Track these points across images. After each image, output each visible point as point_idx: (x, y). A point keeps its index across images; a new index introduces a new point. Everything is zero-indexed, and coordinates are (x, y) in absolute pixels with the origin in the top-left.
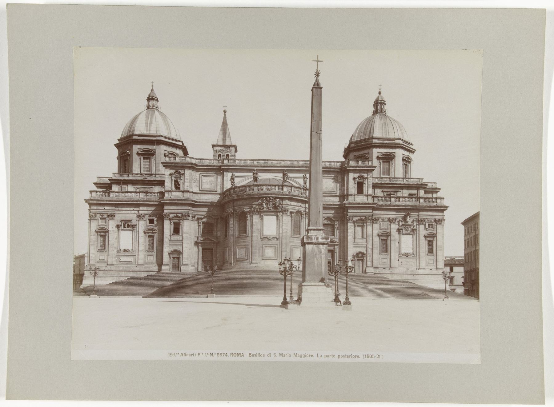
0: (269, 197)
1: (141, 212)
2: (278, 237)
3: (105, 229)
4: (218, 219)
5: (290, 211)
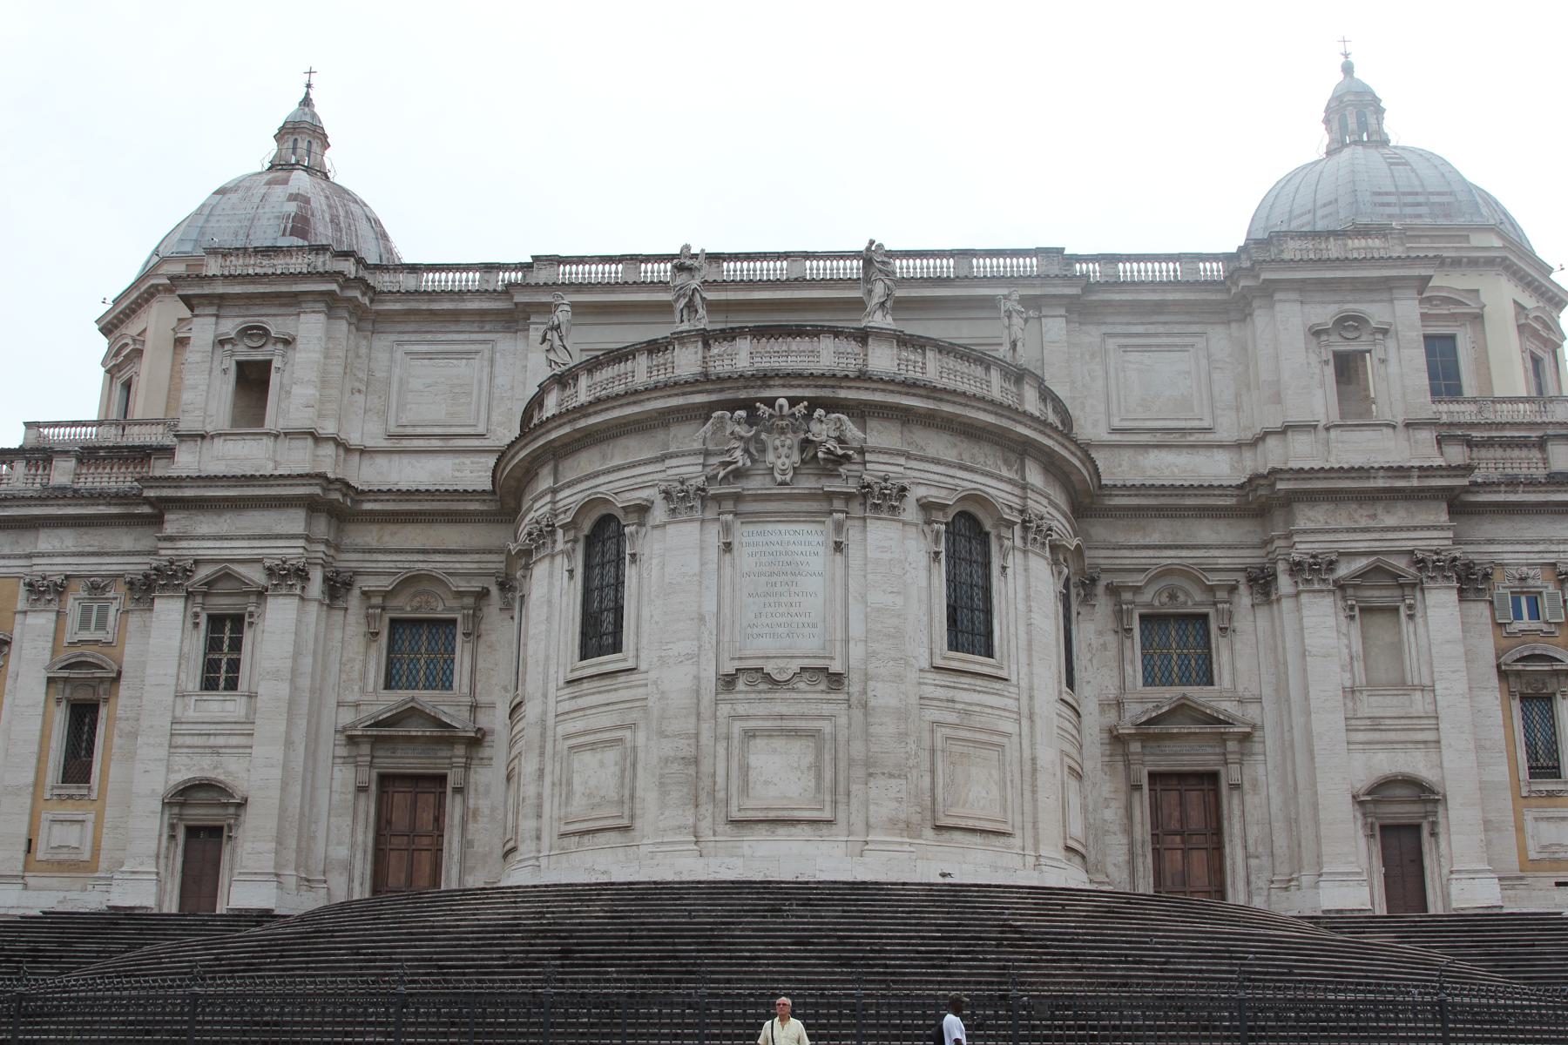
0: (770, 402)
1: (42, 566)
2: (836, 667)
4: (484, 594)
5: (921, 492)
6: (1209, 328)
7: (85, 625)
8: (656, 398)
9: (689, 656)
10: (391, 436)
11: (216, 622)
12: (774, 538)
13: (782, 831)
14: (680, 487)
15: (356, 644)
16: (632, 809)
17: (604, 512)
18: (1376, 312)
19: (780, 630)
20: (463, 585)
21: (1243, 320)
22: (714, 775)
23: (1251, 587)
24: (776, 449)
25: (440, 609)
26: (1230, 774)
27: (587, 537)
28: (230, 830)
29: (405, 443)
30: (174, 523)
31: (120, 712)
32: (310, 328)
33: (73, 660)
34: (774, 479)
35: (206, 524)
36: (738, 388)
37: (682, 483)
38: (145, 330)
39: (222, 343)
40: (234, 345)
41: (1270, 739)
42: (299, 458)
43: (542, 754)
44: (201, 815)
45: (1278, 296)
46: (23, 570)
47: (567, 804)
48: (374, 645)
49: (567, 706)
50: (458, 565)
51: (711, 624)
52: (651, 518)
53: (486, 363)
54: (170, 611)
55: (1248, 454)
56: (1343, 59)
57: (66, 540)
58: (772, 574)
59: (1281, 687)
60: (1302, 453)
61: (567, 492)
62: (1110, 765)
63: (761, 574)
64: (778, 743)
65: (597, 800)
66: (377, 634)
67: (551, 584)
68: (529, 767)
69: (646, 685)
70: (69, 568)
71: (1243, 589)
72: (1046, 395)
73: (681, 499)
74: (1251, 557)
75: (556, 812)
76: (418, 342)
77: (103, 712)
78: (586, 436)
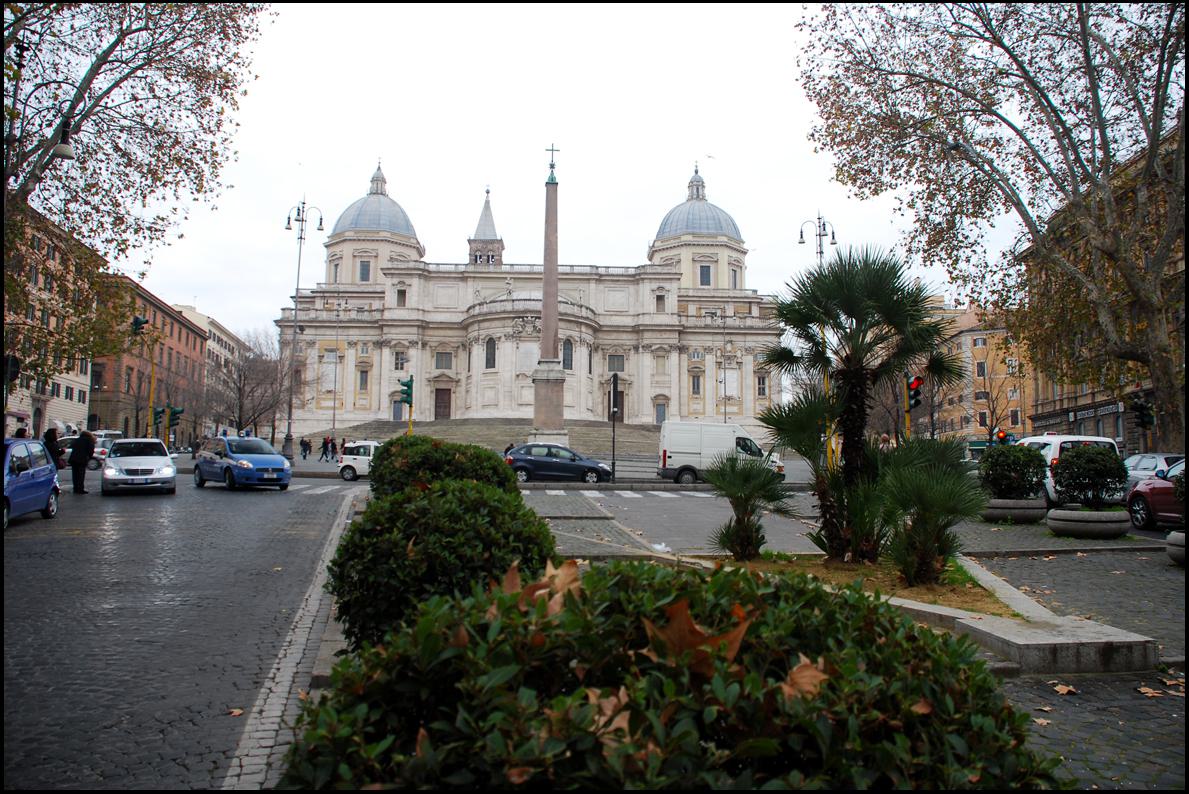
1: (351, 338)
4: (458, 347)
11: (397, 354)
15: (430, 358)
18: (667, 285)
20: (452, 345)
26: (626, 392)
30: (386, 330)
32: (415, 282)
35: (393, 330)
41: (635, 385)
42: (414, 316)
54: (386, 351)
56: (695, 168)
57: (356, 331)
59: (638, 373)
60: (646, 320)
62: (599, 389)
68: (473, 390)
72: (587, 308)
73: (508, 337)
74: (634, 343)
77: (369, 373)
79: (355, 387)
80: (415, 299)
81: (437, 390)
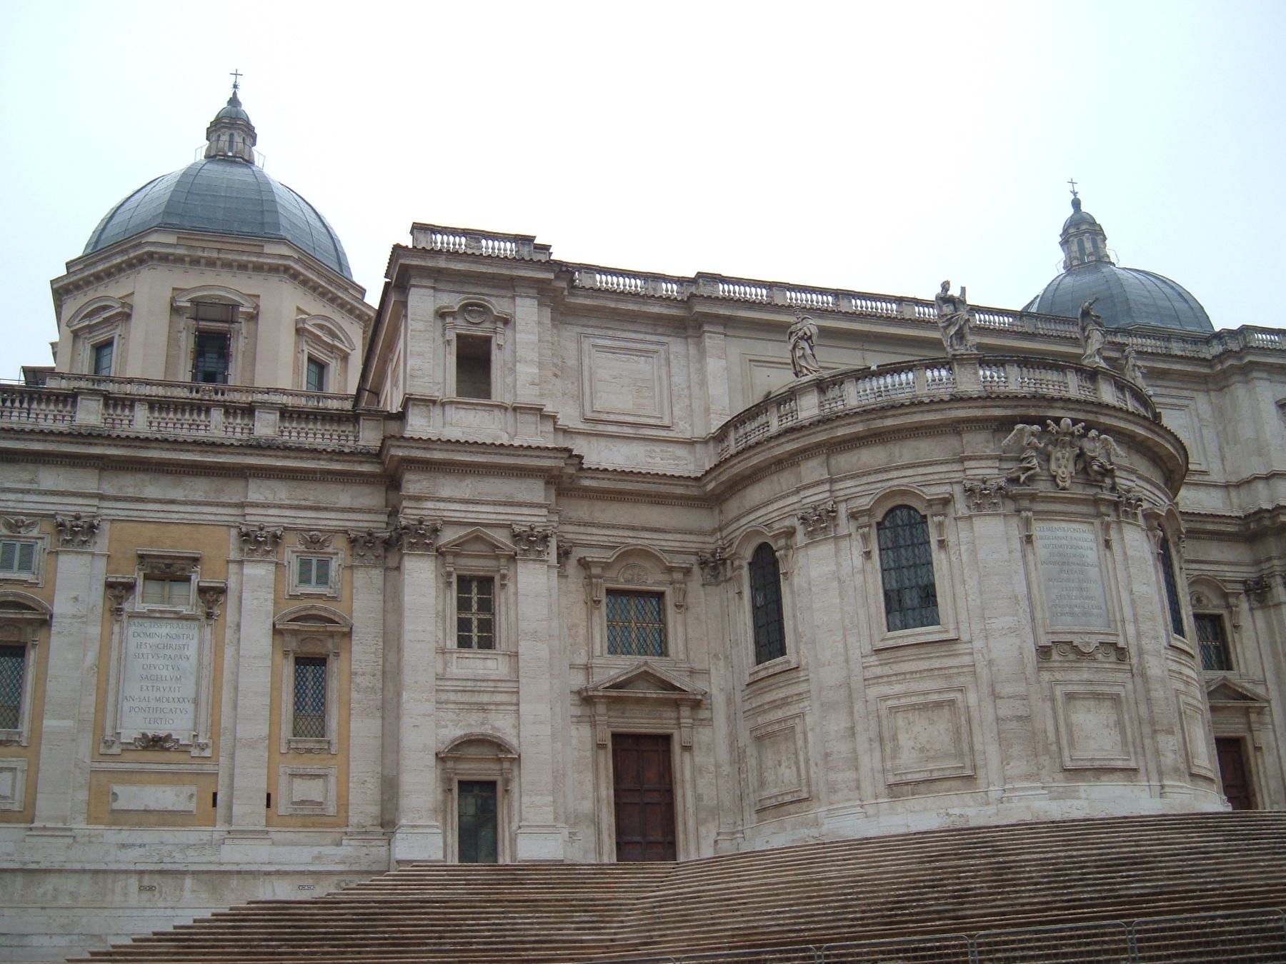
0: (1057, 421)
1: (255, 517)
2: (1121, 644)
3: (29, 608)
4: (687, 571)
6: (1194, 394)
7: (304, 579)
8: (957, 408)
9: (1012, 630)
10: (587, 420)
11: (464, 582)
12: (1060, 534)
13: (1104, 778)
14: (983, 486)
15: (579, 612)
16: (974, 760)
17: (899, 502)
19: (1076, 610)
21: (1221, 389)
22: (1045, 732)
23: (1248, 596)
24: (1058, 459)
25: (649, 582)
27: (879, 524)
28: (507, 782)
29: (600, 428)
30: (413, 483)
31: (355, 667)
32: (527, 311)
33: (304, 613)
34: (1058, 486)
35: (449, 487)
36: (1028, 407)
37: (984, 482)
38: (133, 293)
39: (441, 315)
40: (454, 319)
42: (532, 434)
43: (851, 713)
44: (475, 769)
45: (1255, 374)
46: (232, 519)
47: (893, 758)
48: (596, 613)
49: (879, 671)
50: (663, 543)
51: (1024, 604)
52: (952, 511)
53: (663, 362)
55: (1233, 493)
57: (280, 492)
58: (1064, 564)
61: (849, 483)
63: (1055, 563)
64: (1092, 703)
65: (932, 753)
66: (600, 601)
67: (838, 564)
69: (972, 654)
70: (287, 520)
71: (1243, 597)
73: (979, 496)
74: (1248, 573)
75: (878, 766)
76: (600, 337)
77: (334, 666)
78: (871, 436)
79: (273, 723)
80: (527, 371)
81: (615, 736)
